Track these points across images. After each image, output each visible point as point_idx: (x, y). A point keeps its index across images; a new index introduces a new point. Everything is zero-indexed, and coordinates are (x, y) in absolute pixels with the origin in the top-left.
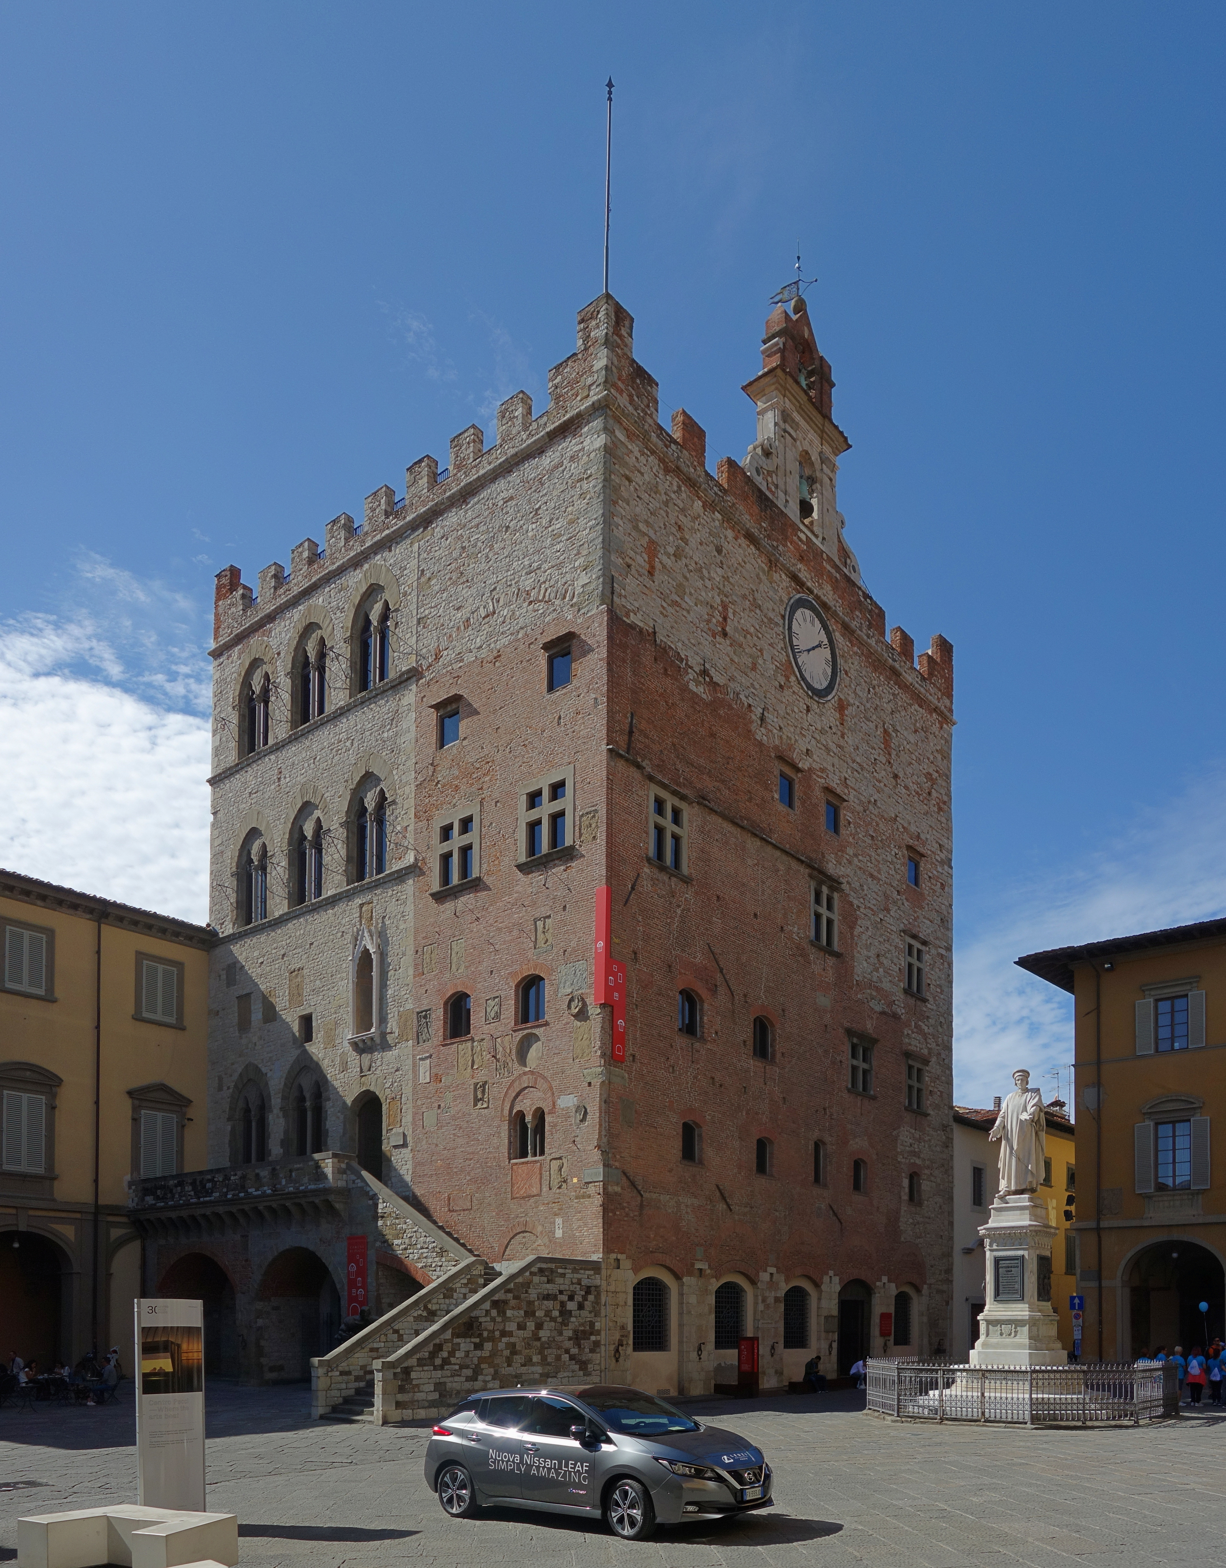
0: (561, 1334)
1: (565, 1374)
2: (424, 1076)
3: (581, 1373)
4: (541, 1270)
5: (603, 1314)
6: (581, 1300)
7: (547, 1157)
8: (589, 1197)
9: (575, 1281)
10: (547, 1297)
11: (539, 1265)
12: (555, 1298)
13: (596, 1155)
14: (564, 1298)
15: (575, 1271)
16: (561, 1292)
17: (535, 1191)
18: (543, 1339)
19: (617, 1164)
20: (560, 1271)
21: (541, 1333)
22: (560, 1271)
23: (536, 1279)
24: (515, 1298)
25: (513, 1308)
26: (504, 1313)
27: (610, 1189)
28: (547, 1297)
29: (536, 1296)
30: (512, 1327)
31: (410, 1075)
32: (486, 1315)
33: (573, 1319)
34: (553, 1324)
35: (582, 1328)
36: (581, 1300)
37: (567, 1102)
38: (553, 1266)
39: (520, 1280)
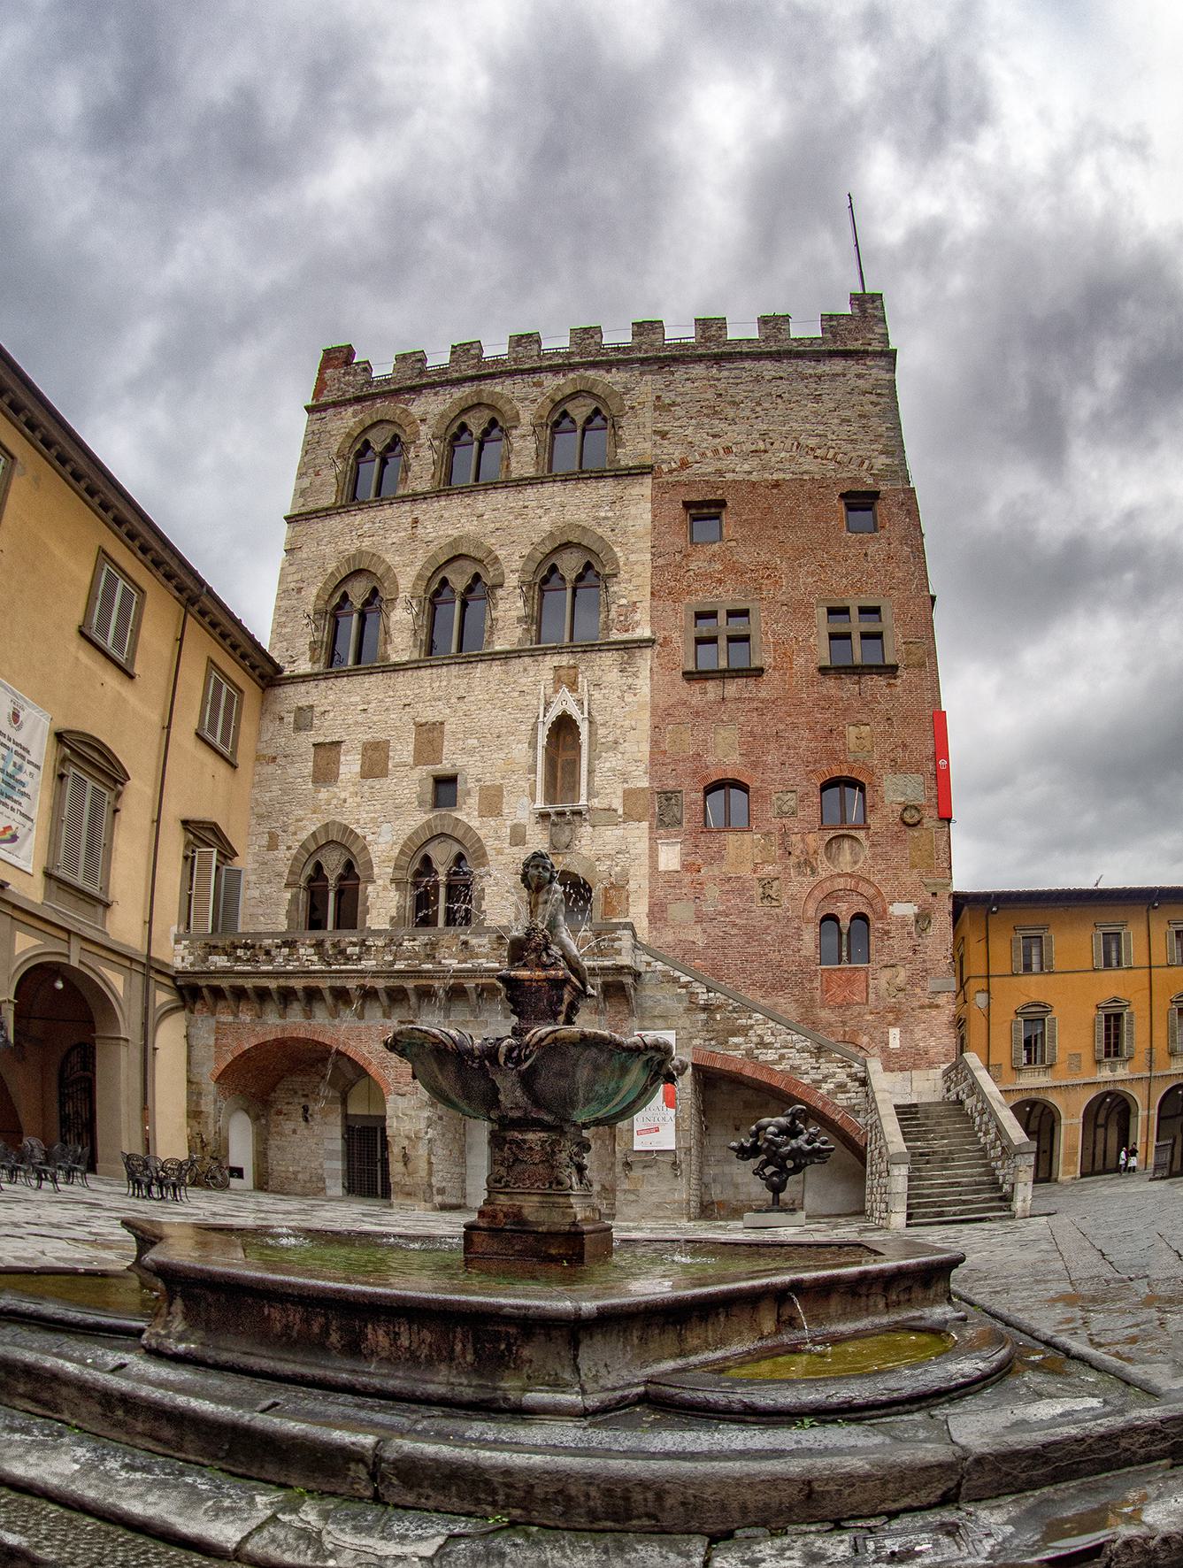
8: (937, 1006)
37: (904, 910)
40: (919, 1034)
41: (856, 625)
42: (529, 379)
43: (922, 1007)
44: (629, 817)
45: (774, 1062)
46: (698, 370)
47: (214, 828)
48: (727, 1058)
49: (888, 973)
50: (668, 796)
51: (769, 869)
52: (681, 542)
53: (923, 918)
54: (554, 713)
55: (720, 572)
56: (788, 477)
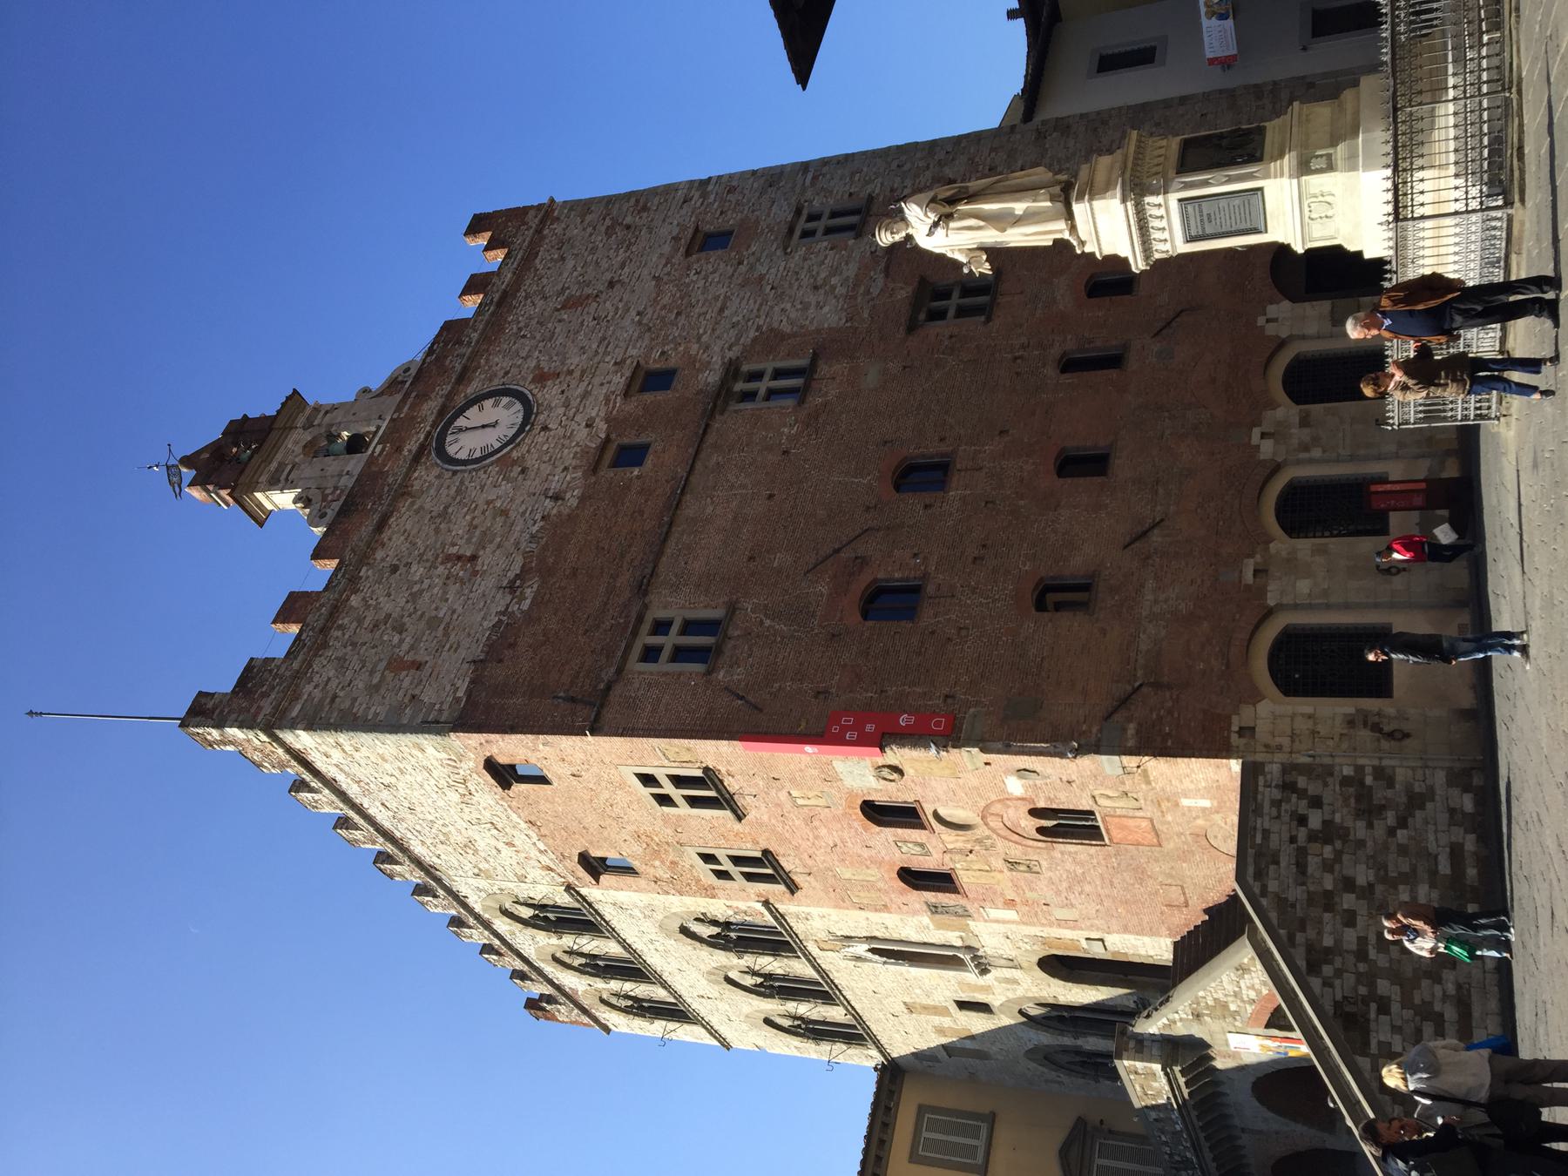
0: (1361, 844)
1: (1431, 837)
2: (1011, 915)
3: (1429, 805)
4: (1259, 875)
5: (1327, 761)
6: (1304, 803)
7: (1095, 808)
9: (1274, 812)
10: (1301, 867)
11: (1250, 880)
12: (1302, 853)
13: (1087, 763)
14: (1302, 834)
15: (1258, 811)
16: (1293, 840)
17: (1145, 824)
18: (1371, 878)
19: (1095, 730)
20: (1258, 840)
21: (1361, 880)
22: (1258, 840)
23: (1273, 886)
24: (1303, 929)
25: (1320, 933)
26: (1328, 951)
27: (1130, 743)
28: (1301, 867)
29: (1300, 889)
30: (1350, 937)
31: (1013, 927)
32: (1331, 986)
33: (1338, 818)
34: (1345, 857)
35: (1353, 800)
36: (1304, 803)
37: (1015, 786)
38: (1251, 852)
39: (1273, 916)
40: (1192, 787)
41: (668, 788)
42: (508, 937)
43: (1148, 783)
44: (965, 929)
45: (1258, 992)
46: (418, 849)
47: (1064, 1153)
48: (1256, 1014)
49: (1101, 801)
50: (934, 909)
51: (998, 863)
52: (641, 882)
53: (1022, 772)
54: (870, 955)
55: (663, 862)
56: (514, 817)
